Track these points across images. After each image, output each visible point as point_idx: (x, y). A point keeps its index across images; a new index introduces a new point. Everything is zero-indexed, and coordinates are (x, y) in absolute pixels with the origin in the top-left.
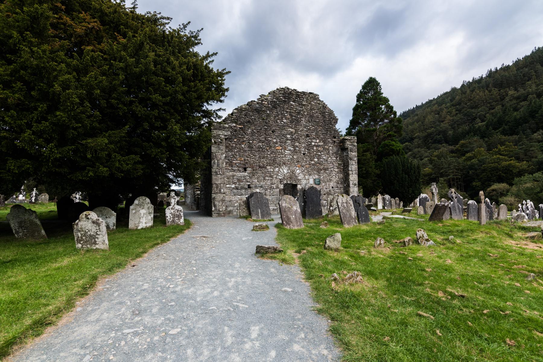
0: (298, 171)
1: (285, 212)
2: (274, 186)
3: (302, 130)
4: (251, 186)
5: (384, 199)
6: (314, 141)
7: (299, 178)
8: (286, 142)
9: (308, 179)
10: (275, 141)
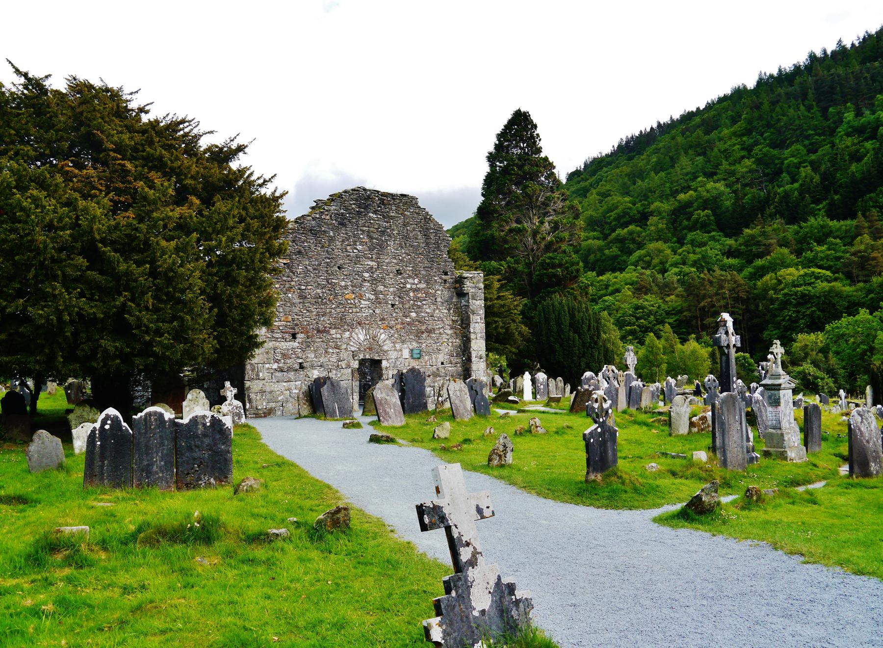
0: (383, 335)
1: (381, 404)
2: (343, 364)
3: (389, 262)
4: (305, 365)
5: (534, 381)
6: (410, 281)
7: (385, 348)
8: (361, 286)
9: (401, 350)
10: (343, 284)
